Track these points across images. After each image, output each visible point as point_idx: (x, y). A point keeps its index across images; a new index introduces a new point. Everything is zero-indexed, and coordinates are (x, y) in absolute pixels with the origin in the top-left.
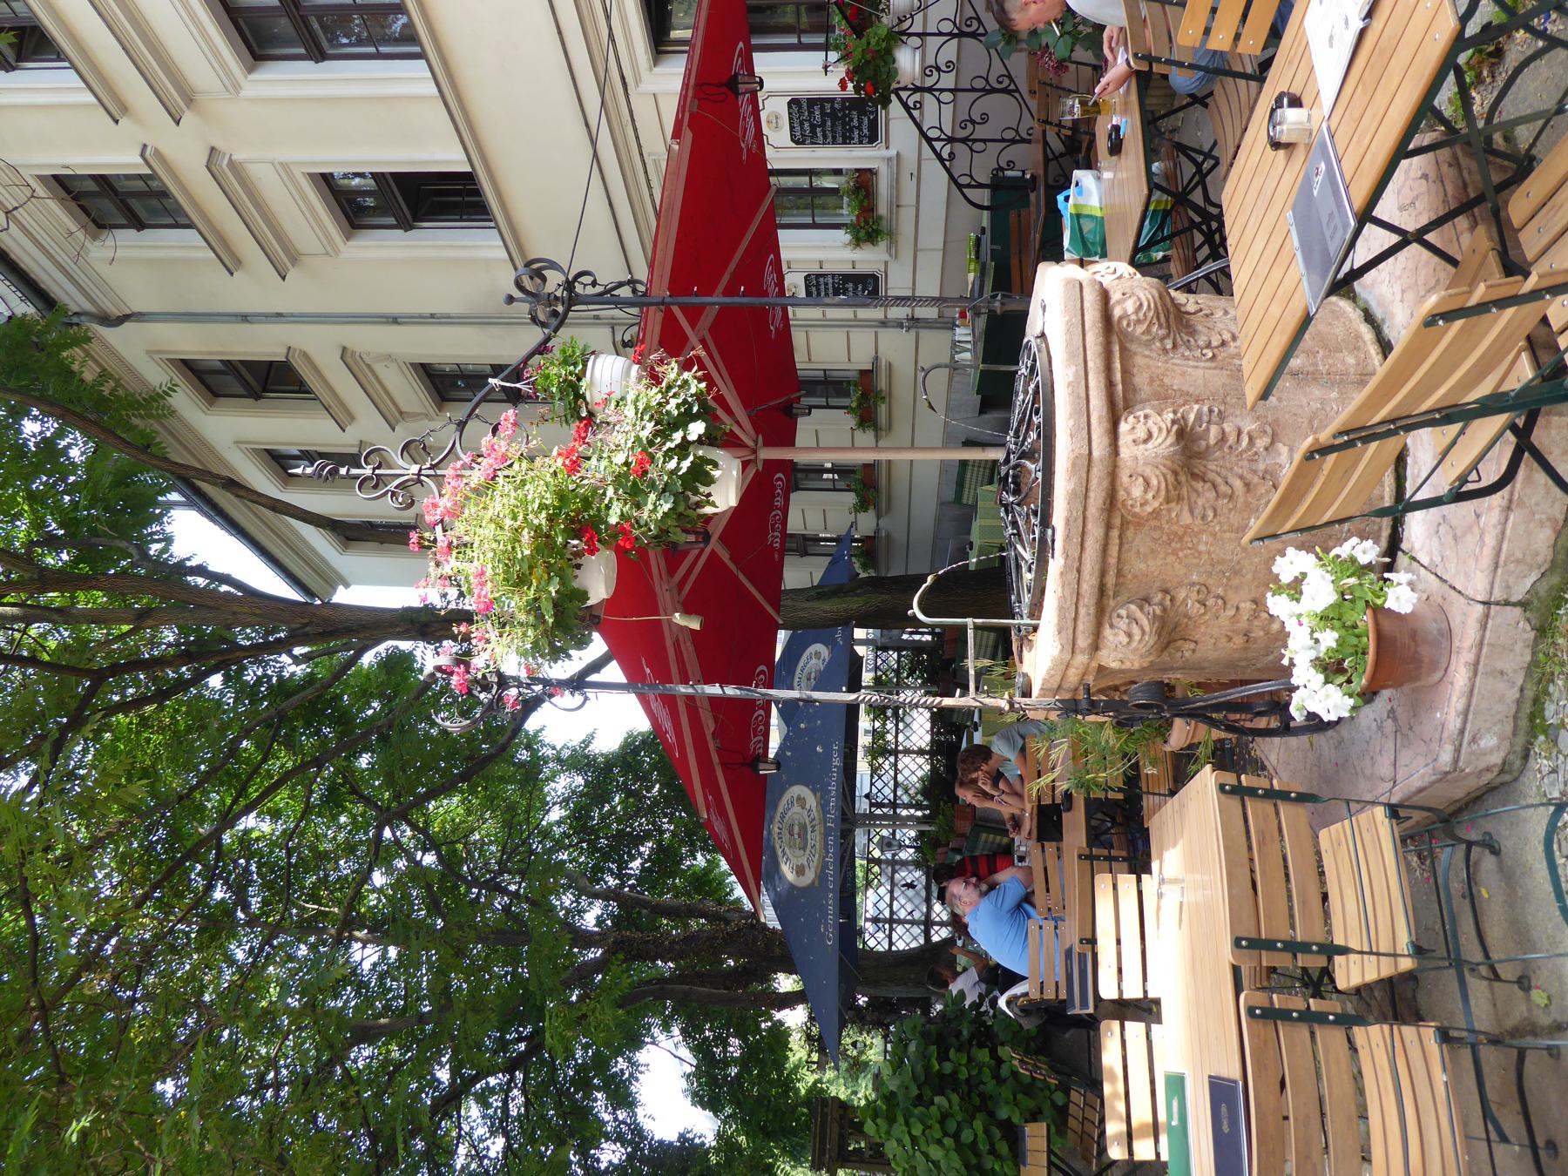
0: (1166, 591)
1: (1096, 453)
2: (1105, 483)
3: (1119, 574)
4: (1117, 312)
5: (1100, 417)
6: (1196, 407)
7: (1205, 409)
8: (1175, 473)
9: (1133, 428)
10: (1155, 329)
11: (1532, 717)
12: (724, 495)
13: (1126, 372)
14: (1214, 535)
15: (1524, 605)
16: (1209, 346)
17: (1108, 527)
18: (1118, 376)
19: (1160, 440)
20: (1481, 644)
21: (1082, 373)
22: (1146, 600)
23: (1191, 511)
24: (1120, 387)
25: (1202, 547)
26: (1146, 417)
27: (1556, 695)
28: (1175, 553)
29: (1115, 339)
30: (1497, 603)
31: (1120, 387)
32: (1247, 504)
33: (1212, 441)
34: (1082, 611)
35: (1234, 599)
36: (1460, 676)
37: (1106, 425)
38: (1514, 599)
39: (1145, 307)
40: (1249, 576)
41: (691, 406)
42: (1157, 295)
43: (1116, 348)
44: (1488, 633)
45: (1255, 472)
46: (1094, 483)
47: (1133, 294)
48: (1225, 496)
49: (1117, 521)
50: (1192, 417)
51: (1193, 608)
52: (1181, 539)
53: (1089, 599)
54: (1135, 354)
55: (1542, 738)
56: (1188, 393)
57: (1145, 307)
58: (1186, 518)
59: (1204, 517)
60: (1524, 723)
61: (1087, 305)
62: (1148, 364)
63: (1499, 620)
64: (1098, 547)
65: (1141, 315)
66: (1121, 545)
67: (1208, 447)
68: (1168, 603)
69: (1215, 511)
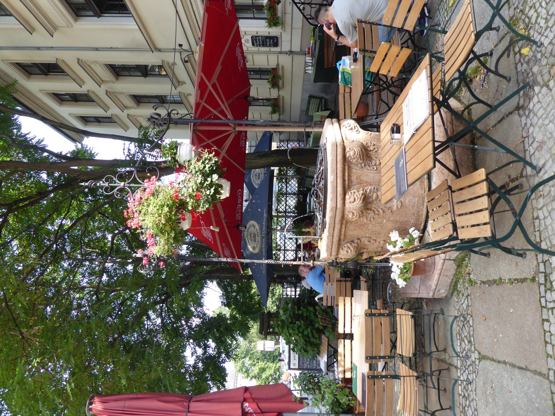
0: (358, 239)
1: (338, 206)
2: (341, 214)
3: (345, 235)
4: (348, 155)
5: (340, 194)
6: (370, 187)
7: (373, 188)
8: (362, 212)
9: (350, 197)
10: (359, 160)
11: (454, 286)
12: (225, 194)
13: (349, 176)
14: (373, 225)
15: (454, 260)
16: (375, 165)
17: (342, 224)
18: (347, 178)
19: (358, 202)
20: (442, 269)
21: (336, 178)
22: (353, 241)
23: (367, 219)
24: (347, 182)
25: (370, 228)
26: (354, 193)
27: (460, 283)
28: (362, 229)
29: (346, 164)
30: (447, 260)
31: (347, 182)
32: (383, 216)
33: (374, 199)
34: (334, 246)
35: (378, 240)
36: (436, 276)
37: (342, 196)
38: (451, 259)
39: (356, 153)
40: (383, 235)
41: (213, 168)
42: (360, 150)
43: (347, 168)
44: (444, 267)
45: (386, 207)
46: (338, 214)
47: (353, 149)
48: (377, 214)
49: (344, 222)
50: (368, 191)
51: (366, 242)
52: (363, 226)
53: (336, 239)
54: (353, 168)
55: (456, 292)
56: (368, 182)
57: (356, 153)
58: (365, 221)
59: (370, 220)
60: (452, 287)
61: (338, 153)
62: (356, 171)
63: (447, 264)
64: (338, 230)
65: (355, 156)
66: (345, 229)
67: (373, 200)
68: (359, 242)
69: (374, 219)
